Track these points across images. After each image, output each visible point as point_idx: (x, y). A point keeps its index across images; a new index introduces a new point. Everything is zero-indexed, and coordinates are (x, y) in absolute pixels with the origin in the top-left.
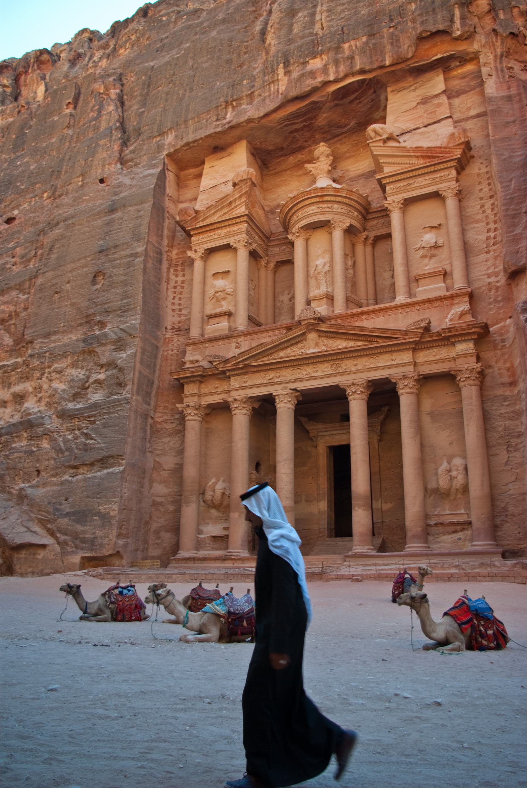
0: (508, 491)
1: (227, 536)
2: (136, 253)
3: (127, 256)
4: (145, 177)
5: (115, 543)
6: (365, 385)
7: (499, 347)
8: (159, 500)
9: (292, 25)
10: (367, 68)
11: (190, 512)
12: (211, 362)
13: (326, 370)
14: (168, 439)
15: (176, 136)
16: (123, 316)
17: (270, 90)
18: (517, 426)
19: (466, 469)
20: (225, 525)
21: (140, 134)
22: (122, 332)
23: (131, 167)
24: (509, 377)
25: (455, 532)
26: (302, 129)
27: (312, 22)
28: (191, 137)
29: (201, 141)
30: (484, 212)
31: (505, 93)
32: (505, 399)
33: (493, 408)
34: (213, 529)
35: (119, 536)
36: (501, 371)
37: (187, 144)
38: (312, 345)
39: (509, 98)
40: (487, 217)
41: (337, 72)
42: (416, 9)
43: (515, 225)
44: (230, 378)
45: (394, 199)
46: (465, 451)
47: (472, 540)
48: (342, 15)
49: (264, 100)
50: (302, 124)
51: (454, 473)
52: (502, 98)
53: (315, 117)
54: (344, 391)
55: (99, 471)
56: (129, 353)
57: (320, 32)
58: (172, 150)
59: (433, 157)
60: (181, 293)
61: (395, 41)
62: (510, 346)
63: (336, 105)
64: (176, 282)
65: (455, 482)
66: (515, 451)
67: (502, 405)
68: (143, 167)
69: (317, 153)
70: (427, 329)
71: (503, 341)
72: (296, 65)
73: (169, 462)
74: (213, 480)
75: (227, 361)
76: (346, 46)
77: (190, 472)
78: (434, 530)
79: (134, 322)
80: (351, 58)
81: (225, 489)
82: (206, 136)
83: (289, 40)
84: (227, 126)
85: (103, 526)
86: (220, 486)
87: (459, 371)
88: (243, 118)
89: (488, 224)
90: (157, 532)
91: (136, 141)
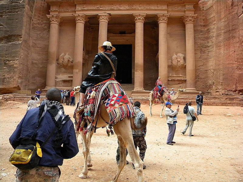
0: (200, 69)
1: (72, 80)
5: (17, 81)
7: (201, 10)
8: (35, 62)
11: (52, 68)
13: (126, 7)
14: (40, 32)
18: (206, 43)
19: (185, 59)
20: (72, 75)
24: (204, 23)
32: (201, 31)
33: (196, 34)
34: (65, 77)
35: (19, 77)
36: (200, 20)
44: (76, 5)
46: (185, 51)
47: (186, 87)
51: (179, 60)
54: (134, 17)
55: (5, 43)
62: (206, 10)
65: (179, 63)
67: (200, 34)
71: (203, 7)
73: (41, 43)
74: (63, 54)
77: (53, 49)
78: (170, 83)
85: (9, 72)
86: (67, 57)
87: (187, 16)
90: (34, 77)
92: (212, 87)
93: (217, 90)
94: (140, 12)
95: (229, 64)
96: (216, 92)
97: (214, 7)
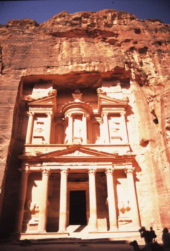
2: (11, 108)
3: (5, 108)
4: (14, 81)
6: (96, 170)
9: (72, 50)
10: (99, 71)
12: (37, 154)
15: (27, 71)
16: (3, 130)
17: (65, 67)
21: (10, 66)
22: (3, 136)
23: (6, 76)
25: (126, 224)
26: (71, 82)
27: (80, 52)
28: (34, 73)
29: (37, 76)
30: (131, 122)
31: (138, 90)
37: (32, 75)
38: (77, 154)
39: (139, 91)
40: (132, 123)
41: (90, 69)
42: (114, 60)
43: (144, 127)
45: (106, 111)
48: (90, 53)
49: (63, 70)
50: (72, 81)
52: (137, 91)
53: (77, 80)
56: (6, 145)
57: (82, 56)
58: (25, 75)
59: (118, 102)
60: (22, 126)
61: (108, 66)
63: (85, 79)
64: (20, 122)
66: (143, 196)
68: (13, 78)
69: (76, 91)
70: (118, 155)
72: (75, 63)
75: (43, 155)
76: (93, 63)
79: (8, 133)
80: (95, 67)
81: (35, 204)
82: (40, 75)
83: (72, 55)
84: (48, 74)
87: (128, 169)
88: (55, 73)
89: (133, 125)
91: (8, 68)
92: (154, 226)
93: (158, 228)
94: (93, 167)
95: (163, 206)
96: (158, 230)
97: (146, 161)
